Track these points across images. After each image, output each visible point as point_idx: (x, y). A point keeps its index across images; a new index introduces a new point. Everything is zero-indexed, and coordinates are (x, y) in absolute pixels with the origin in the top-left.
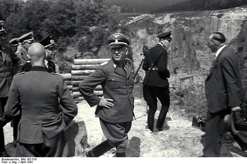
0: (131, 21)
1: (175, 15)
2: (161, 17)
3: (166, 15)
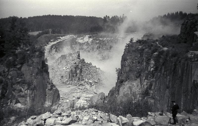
0: (59, 40)
1: (92, 36)
2: (82, 38)
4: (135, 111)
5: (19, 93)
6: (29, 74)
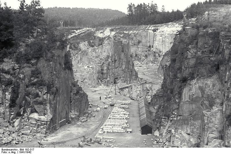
1: (115, 29)
2: (102, 31)
5: (35, 98)
6: (48, 72)
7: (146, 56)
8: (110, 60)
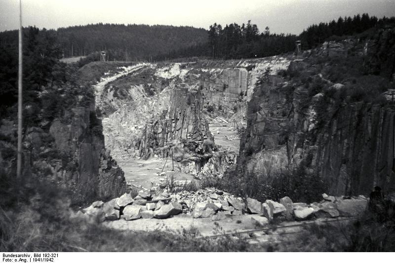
0: (122, 73)
1: (187, 65)
2: (167, 68)
3: (173, 65)
4: (294, 193)
5: (46, 175)
6: (64, 139)
7: (235, 109)
8: (167, 118)
